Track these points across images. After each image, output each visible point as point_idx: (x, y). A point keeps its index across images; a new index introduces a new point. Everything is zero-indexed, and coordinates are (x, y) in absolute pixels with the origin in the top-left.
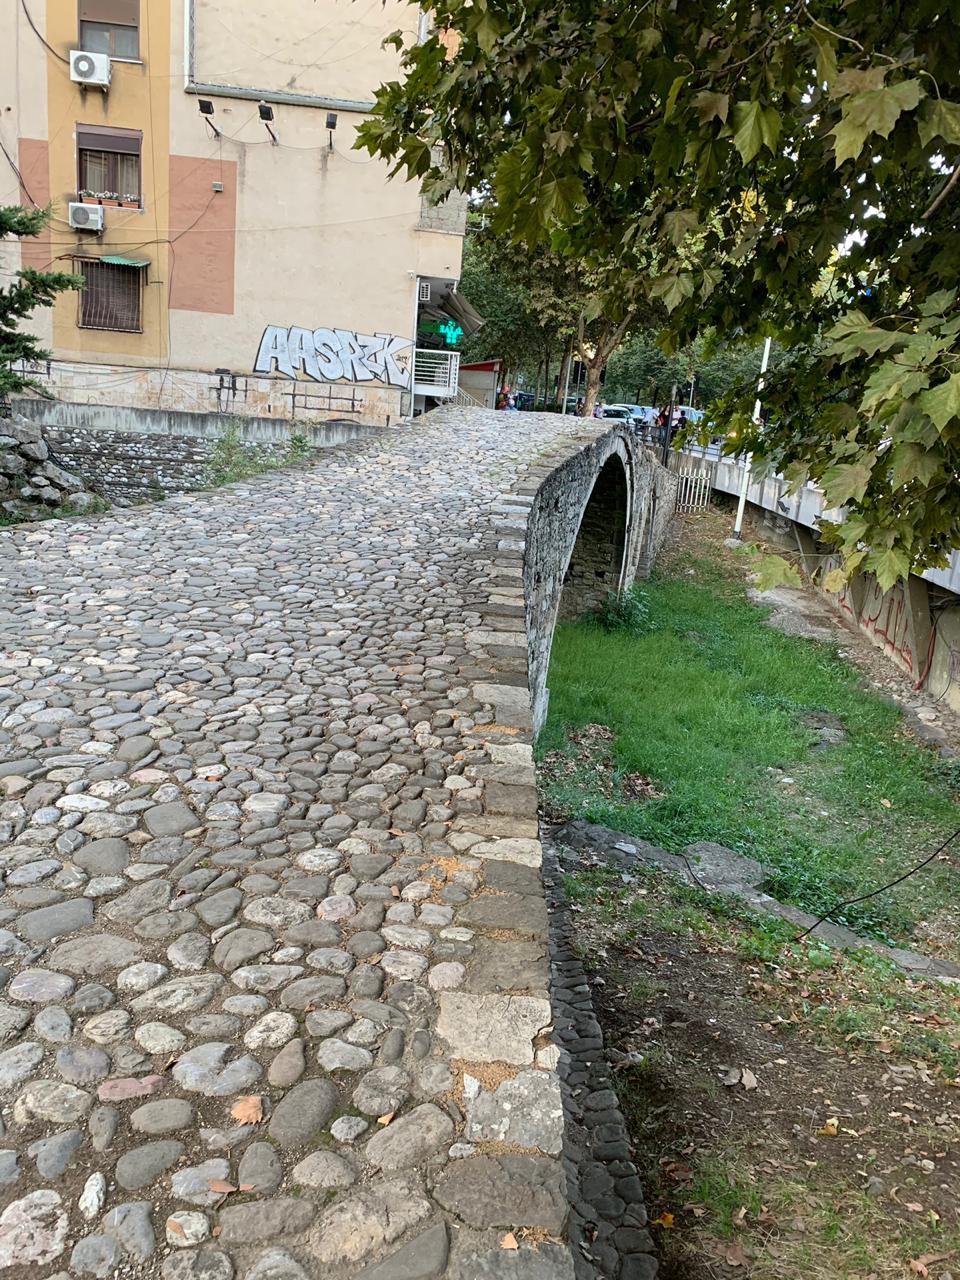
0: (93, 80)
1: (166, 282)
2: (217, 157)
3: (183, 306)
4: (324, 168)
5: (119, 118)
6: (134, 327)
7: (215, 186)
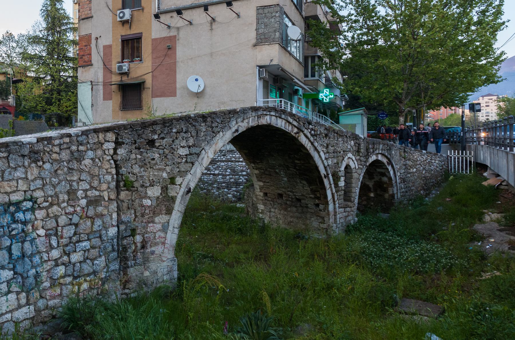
0: (125, 19)
1: (151, 87)
2: (168, 35)
3: (157, 96)
4: (211, 29)
5: (134, 31)
7: (168, 46)
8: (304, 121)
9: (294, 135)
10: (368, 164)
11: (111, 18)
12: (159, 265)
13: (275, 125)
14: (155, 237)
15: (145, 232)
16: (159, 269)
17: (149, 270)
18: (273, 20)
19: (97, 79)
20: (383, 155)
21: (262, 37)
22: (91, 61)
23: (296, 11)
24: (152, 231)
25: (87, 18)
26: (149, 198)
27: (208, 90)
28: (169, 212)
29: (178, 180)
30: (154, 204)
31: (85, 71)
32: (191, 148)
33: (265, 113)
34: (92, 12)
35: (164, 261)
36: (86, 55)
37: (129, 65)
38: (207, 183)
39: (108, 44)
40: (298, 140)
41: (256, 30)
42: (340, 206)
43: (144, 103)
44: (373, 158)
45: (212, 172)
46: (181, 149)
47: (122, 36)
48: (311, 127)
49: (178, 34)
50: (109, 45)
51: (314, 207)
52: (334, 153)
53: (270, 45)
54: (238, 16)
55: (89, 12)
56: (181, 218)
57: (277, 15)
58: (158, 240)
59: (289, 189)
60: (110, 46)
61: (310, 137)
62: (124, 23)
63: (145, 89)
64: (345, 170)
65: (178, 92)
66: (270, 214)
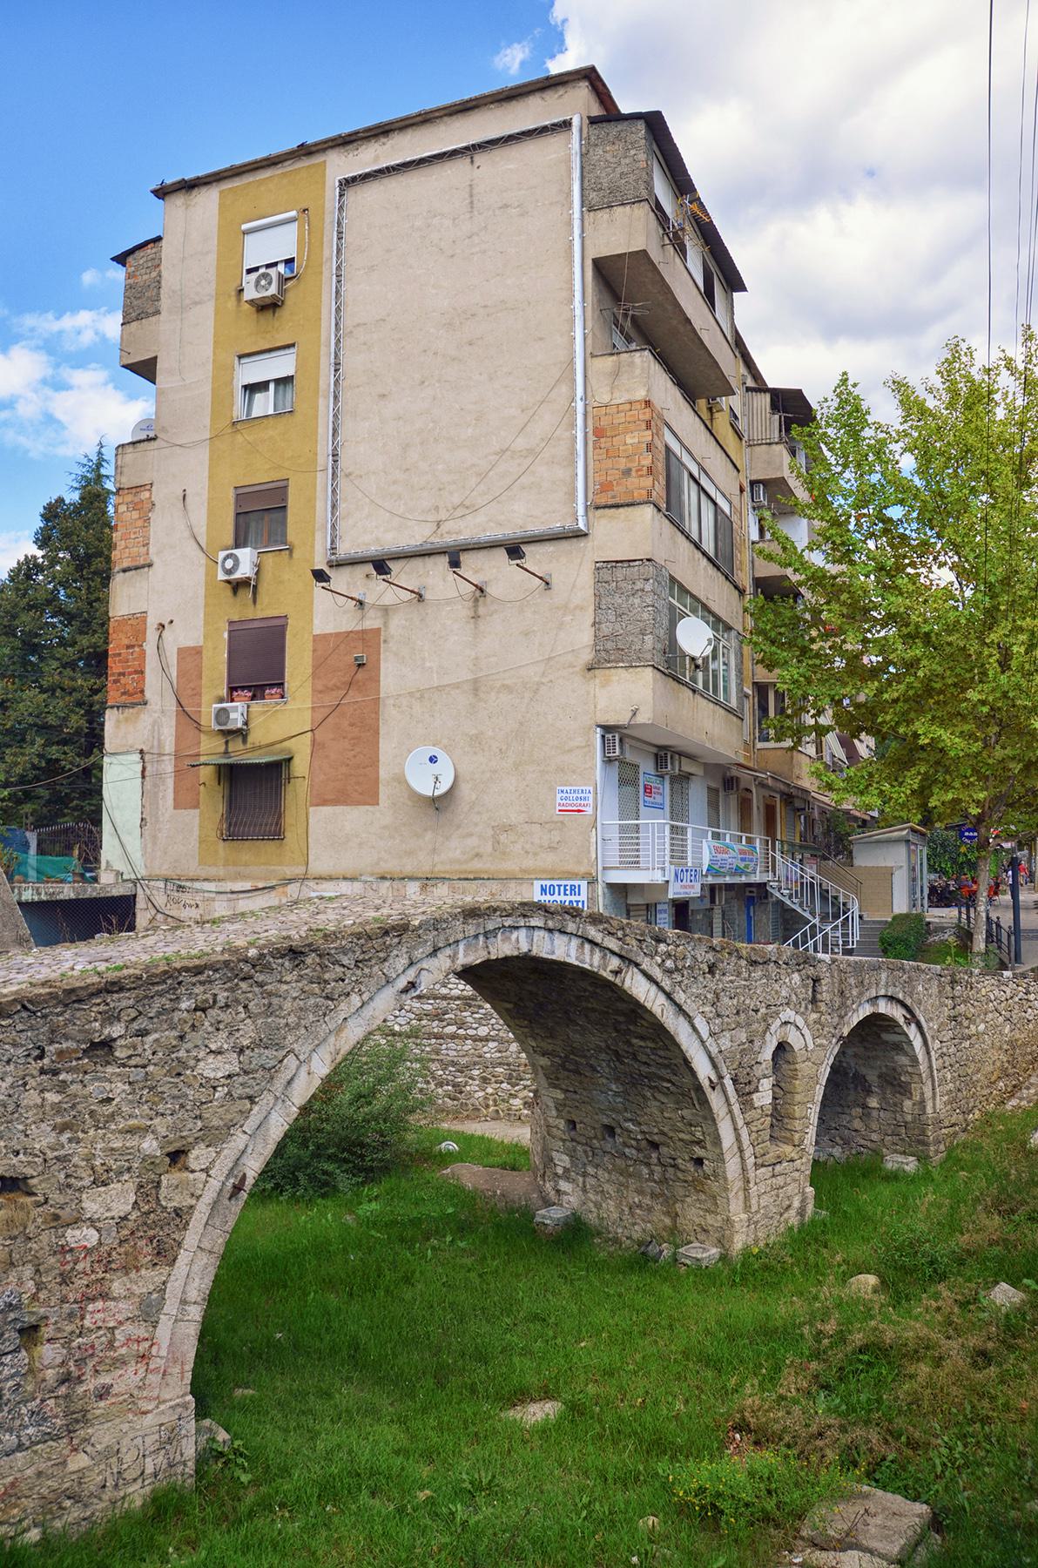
0: (238, 575)
2: (359, 628)
6: (276, 833)
7: (356, 659)
8: (641, 935)
9: (611, 978)
10: (846, 1032)
11: (202, 570)
12: (125, 1427)
13: (545, 956)
14: (111, 1345)
15: (73, 1332)
16: (125, 1442)
17: (89, 1449)
18: (637, 601)
19: (160, 745)
20: (891, 998)
21: (609, 645)
22: (142, 692)
23: (711, 570)
24: (100, 1324)
25: (137, 568)
26: (92, 1222)
27: (465, 790)
28: (165, 1254)
29: (199, 1156)
30: (111, 1240)
31: (127, 720)
32: (247, 1052)
33: (508, 922)
34: (151, 551)
35: (145, 1413)
36: (130, 674)
37: (248, 707)
38: (454, 1064)
39: (191, 644)
40: (625, 991)
41: (594, 624)
42: (760, 1161)
43: (291, 818)
44: (866, 1010)
45: (471, 1032)
46: (211, 1059)
47: (231, 623)
48: (662, 947)
49: (385, 624)
50: (194, 648)
51: (691, 1167)
52: (738, 1013)
53: (631, 670)
54: (547, 584)
55: (143, 550)
56: (212, 1271)
57: (648, 587)
58: (123, 1351)
59: (628, 1115)
60: (197, 652)
61: (659, 980)
62: (237, 586)
63: (292, 781)
64: (773, 1059)
65: (384, 792)
66: (584, 1182)
